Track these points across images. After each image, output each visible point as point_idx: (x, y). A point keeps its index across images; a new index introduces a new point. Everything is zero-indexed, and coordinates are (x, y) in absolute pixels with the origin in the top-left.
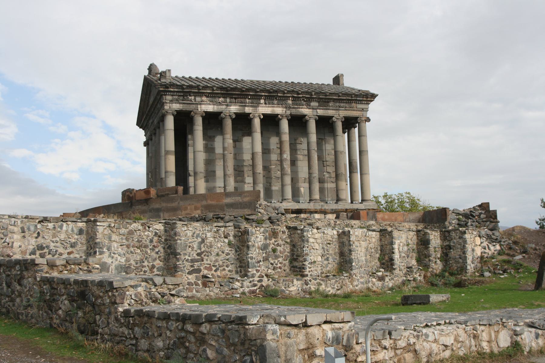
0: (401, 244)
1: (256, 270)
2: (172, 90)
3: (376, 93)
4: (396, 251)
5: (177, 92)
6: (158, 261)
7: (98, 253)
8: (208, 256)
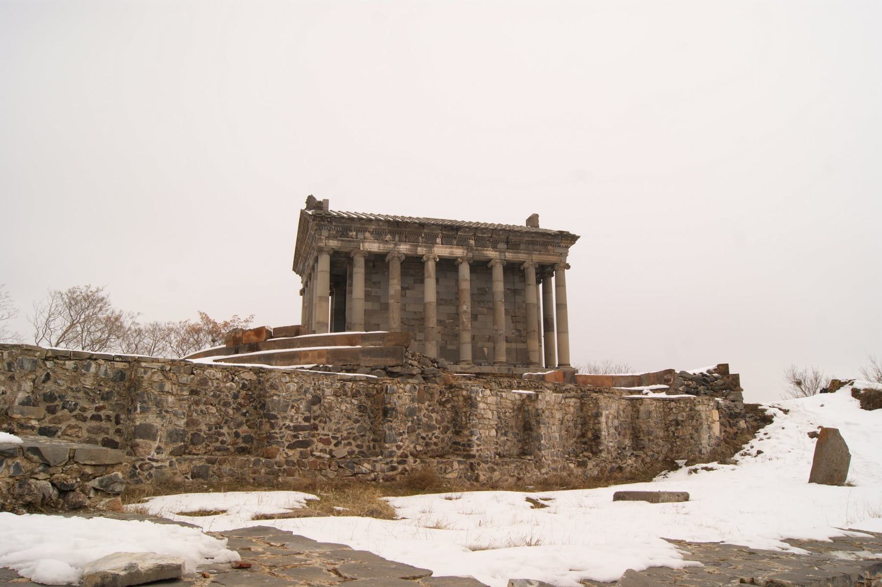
0: (611, 417)
1: (397, 446)
3: (577, 235)
4: (603, 426)
6: (245, 428)
7: (139, 410)
8: (325, 422)
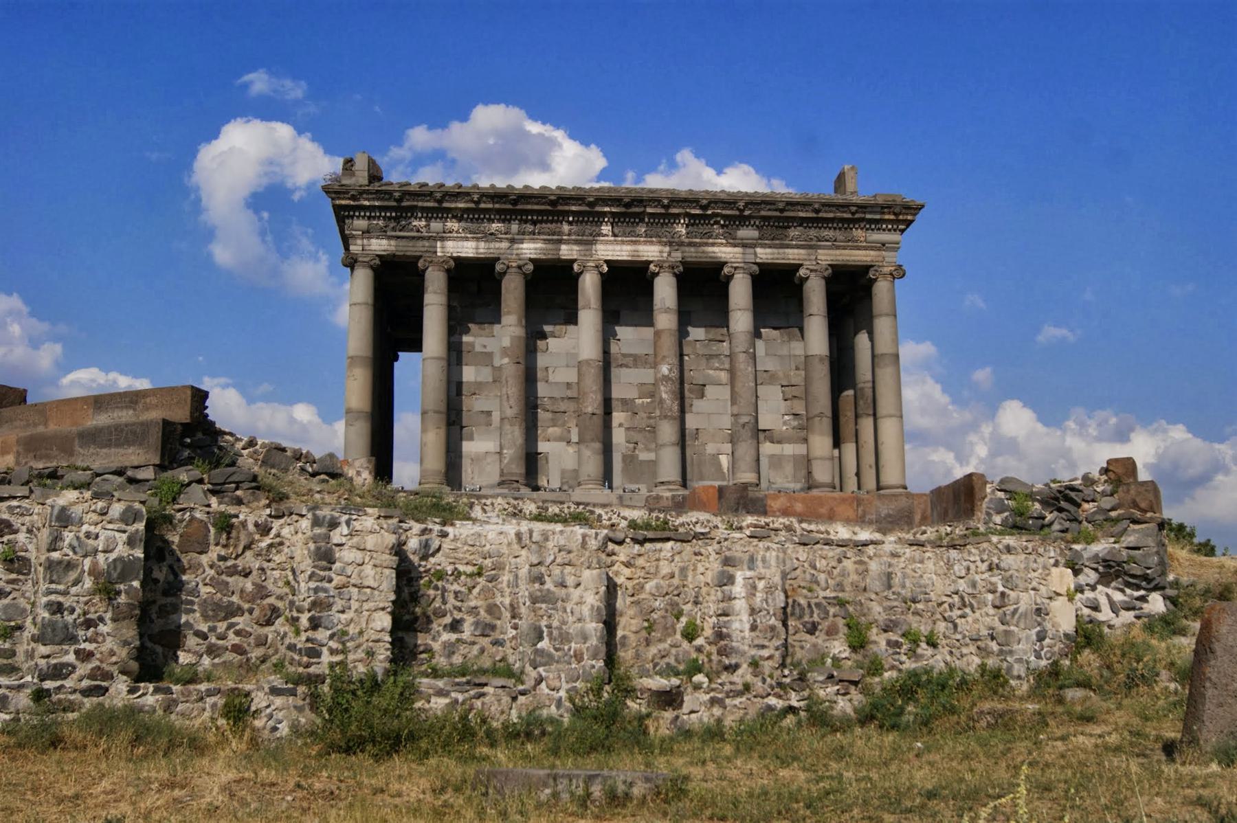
0: (761, 585)
1: (77, 652)
2: (367, 203)
3: (919, 202)
4: (740, 605)
5: (381, 208)
